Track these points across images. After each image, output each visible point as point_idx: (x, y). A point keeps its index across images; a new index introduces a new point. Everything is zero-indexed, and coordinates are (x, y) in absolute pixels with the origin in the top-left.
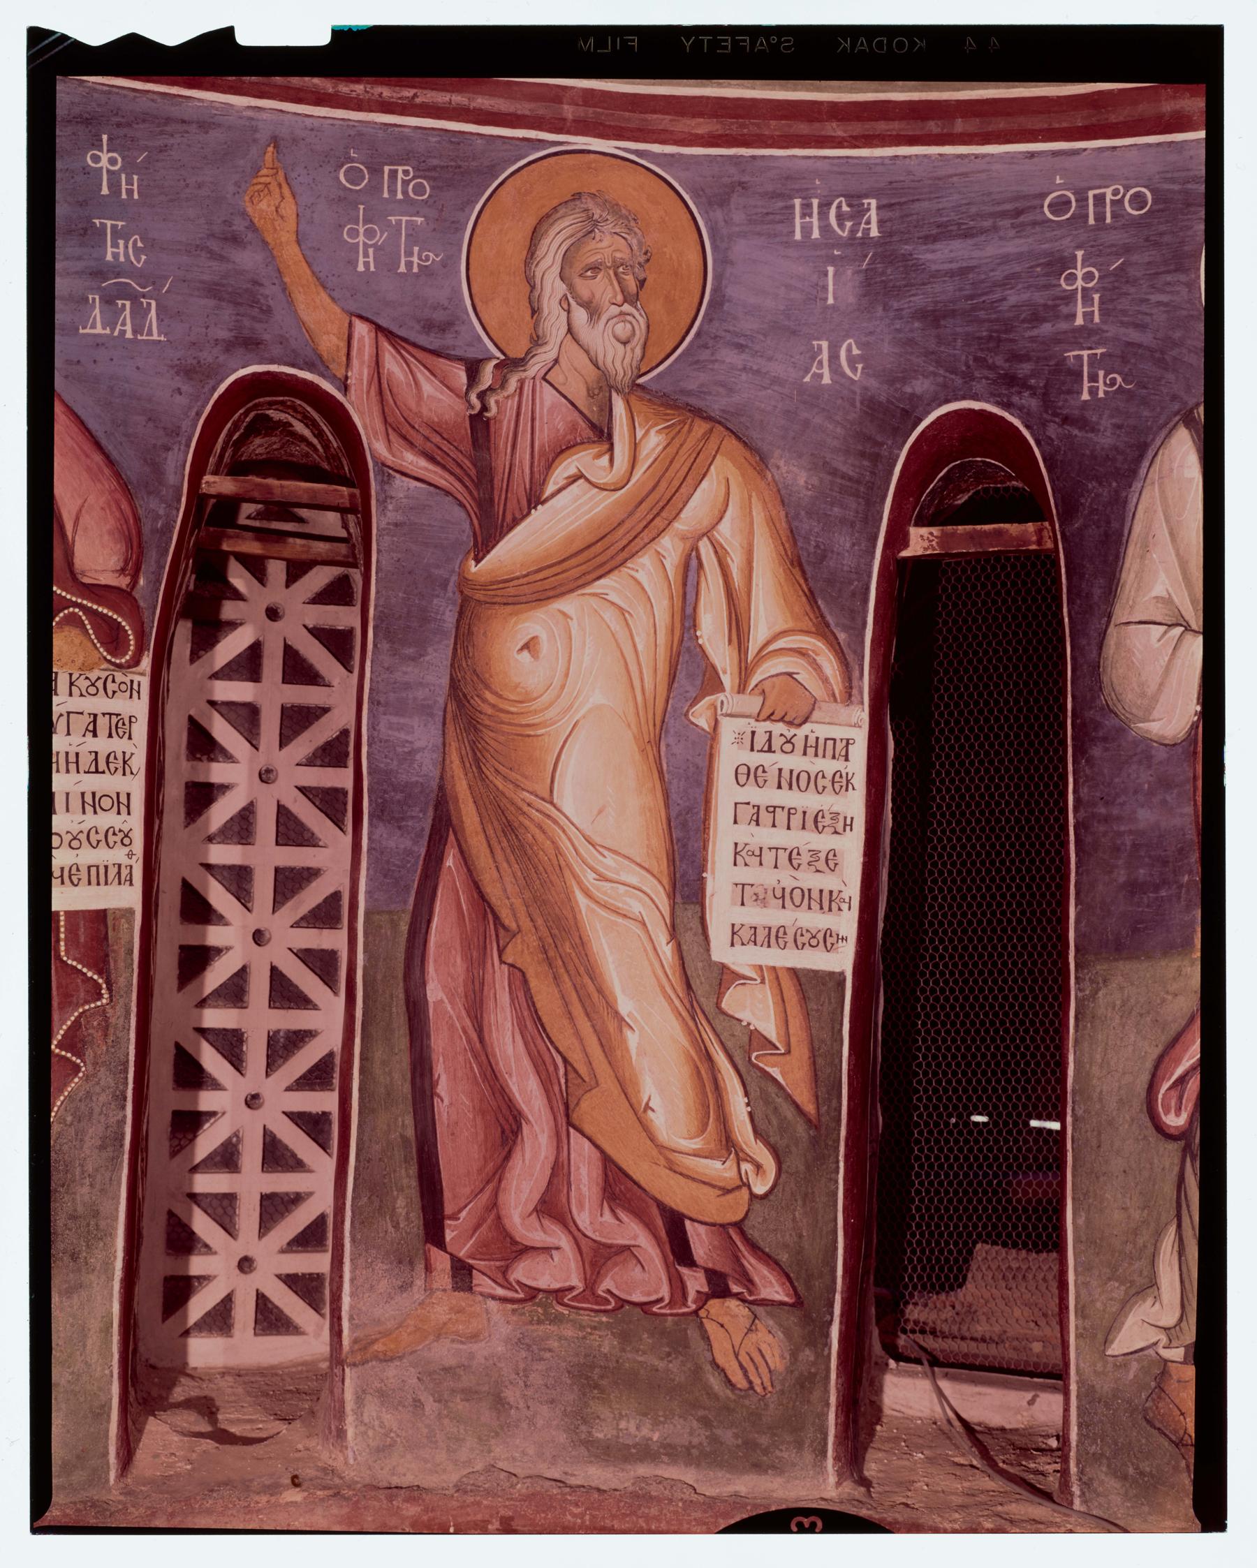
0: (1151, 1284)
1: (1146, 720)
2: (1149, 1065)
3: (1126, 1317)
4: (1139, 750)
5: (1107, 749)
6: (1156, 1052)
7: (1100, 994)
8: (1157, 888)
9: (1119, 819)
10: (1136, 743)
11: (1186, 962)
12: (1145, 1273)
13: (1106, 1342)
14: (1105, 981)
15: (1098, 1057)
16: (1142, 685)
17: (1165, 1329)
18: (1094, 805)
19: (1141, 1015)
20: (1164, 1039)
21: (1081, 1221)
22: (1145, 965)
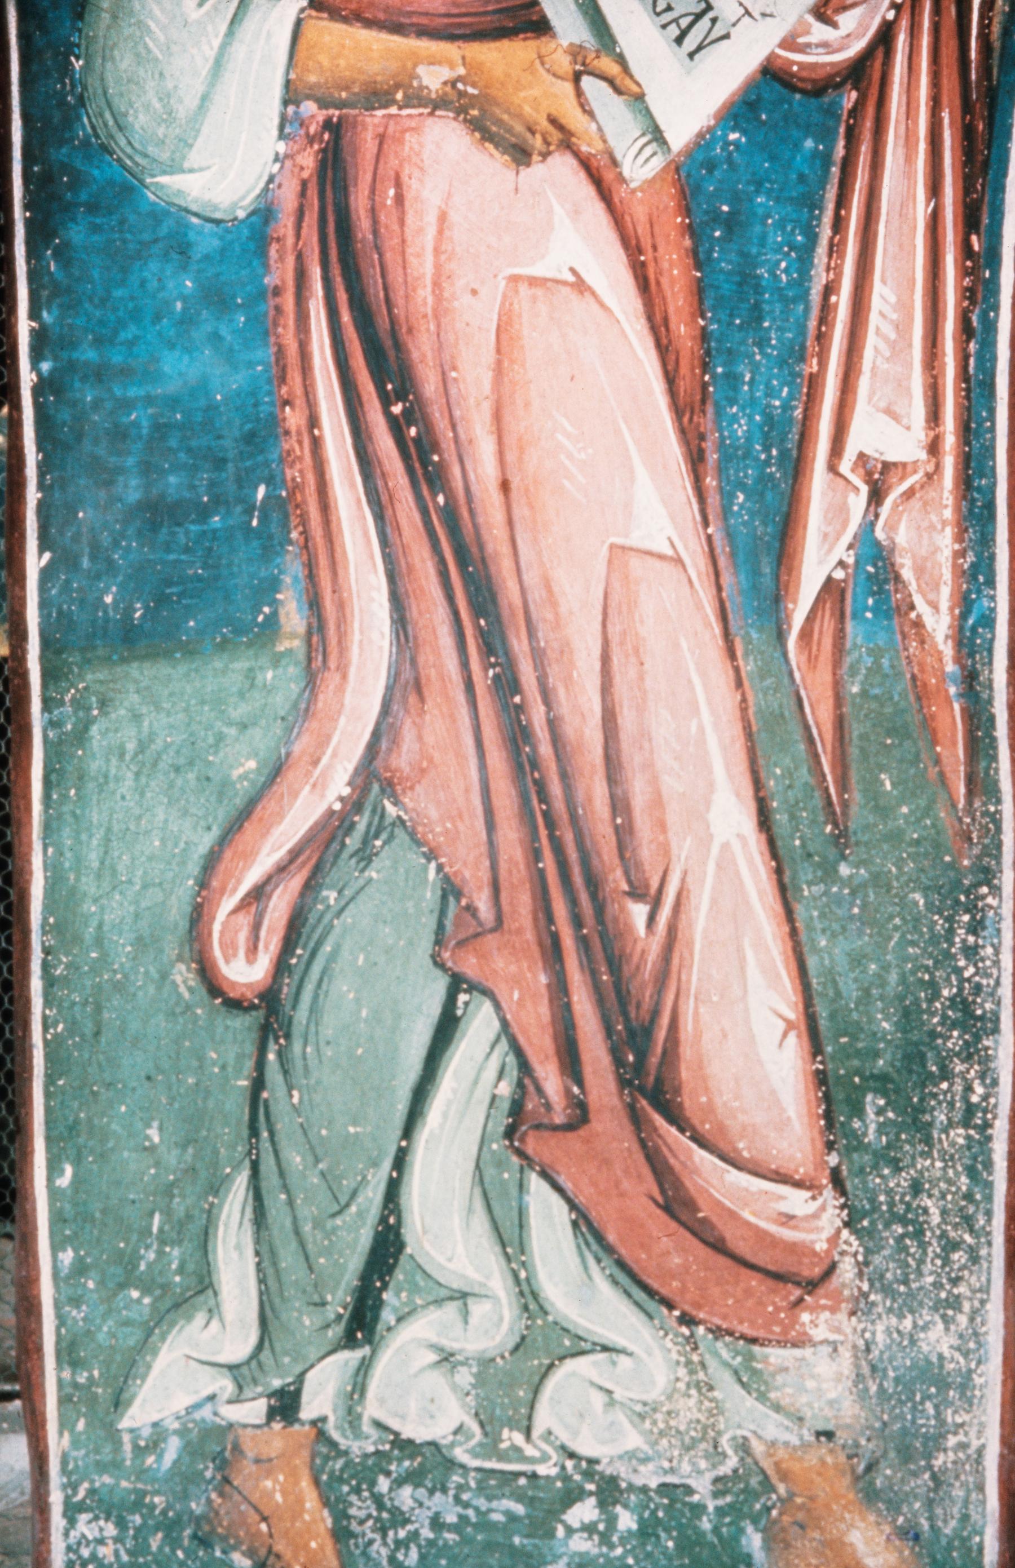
0: (203, 1283)
1: (174, 168)
2: (194, 868)
3: (155, 1353)
4: (163, 230)
5: (96, 229)
6: (206, 842)
7: (94, 730)
8: (204, 513)
9: (125, 372)
10: (156, 216)
11: (264, 661)
12: (191, 1267)
13: (119, 1403)
14: (103, 704)
15: (93, 858)
16: (165, 97)
17: (231, 1368)
18: (73, 345)
19: (177, 769)
20: (222, 815)
21: (64, 1181)
22: (182, 669)
